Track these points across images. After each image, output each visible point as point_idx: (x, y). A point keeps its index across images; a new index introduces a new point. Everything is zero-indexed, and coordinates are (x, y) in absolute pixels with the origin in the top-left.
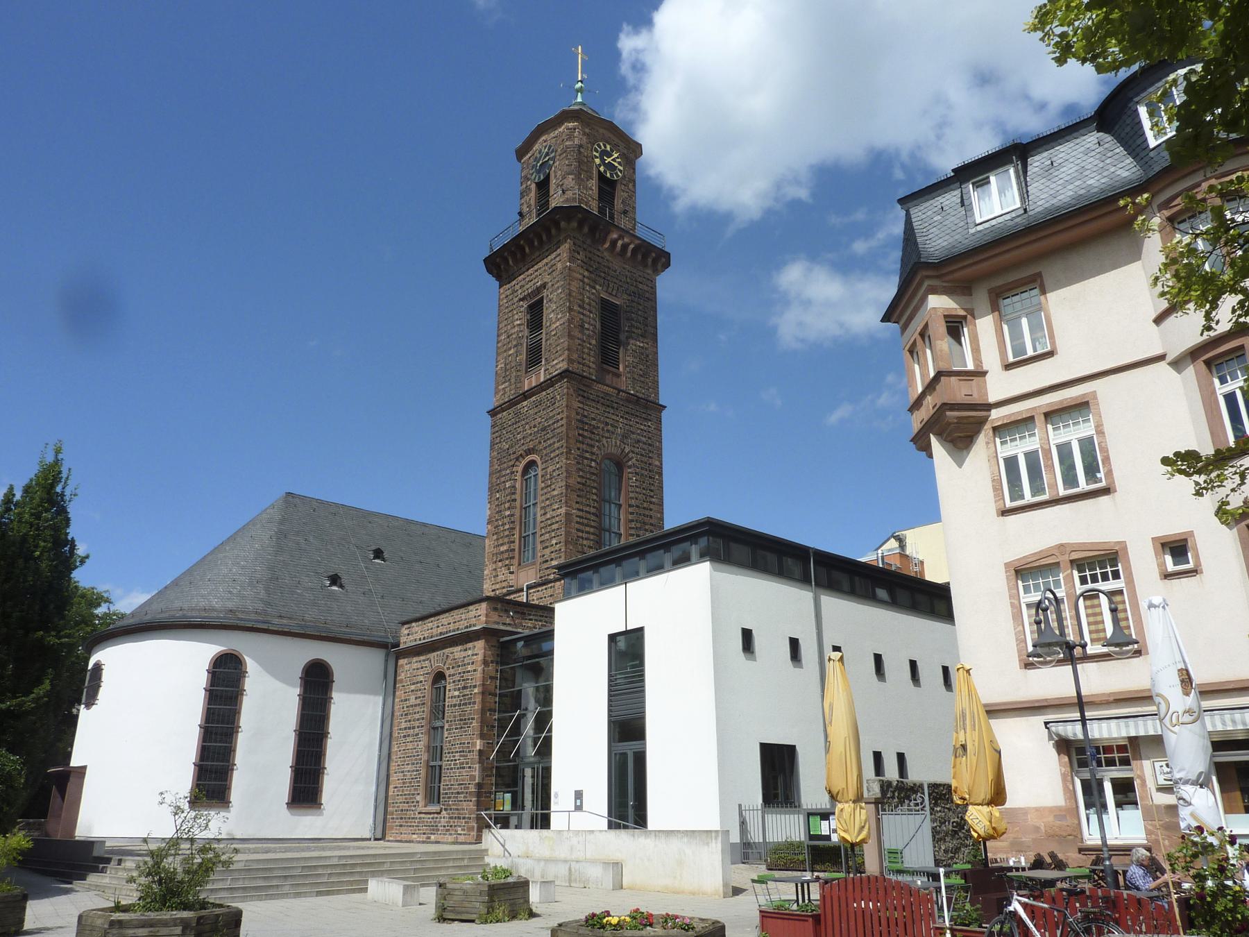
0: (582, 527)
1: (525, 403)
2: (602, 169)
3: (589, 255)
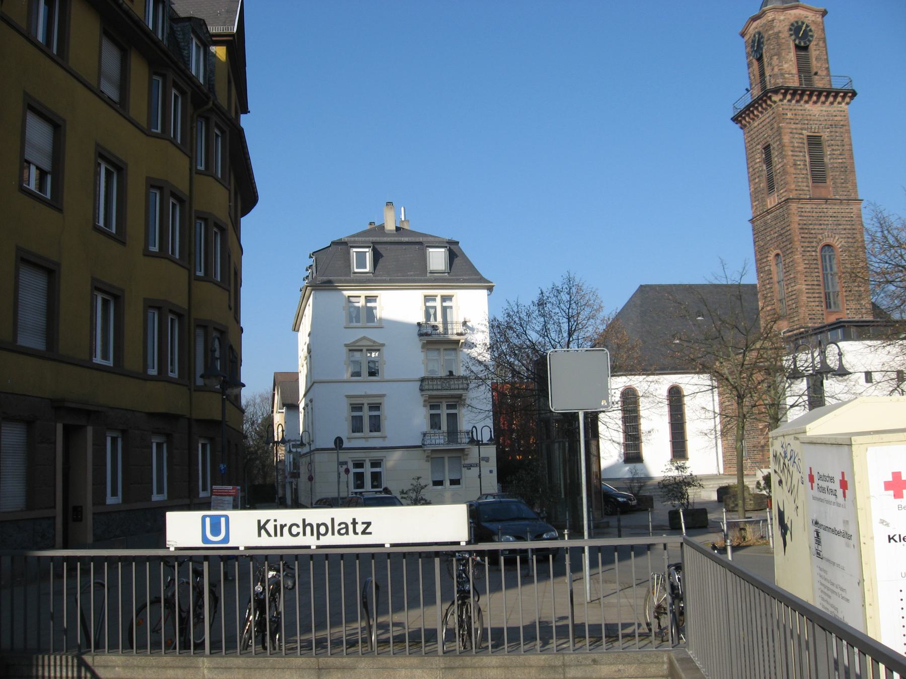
0: (810, 295)
1: (769, 217)
2: (797, 42)
3: (794, 112)
